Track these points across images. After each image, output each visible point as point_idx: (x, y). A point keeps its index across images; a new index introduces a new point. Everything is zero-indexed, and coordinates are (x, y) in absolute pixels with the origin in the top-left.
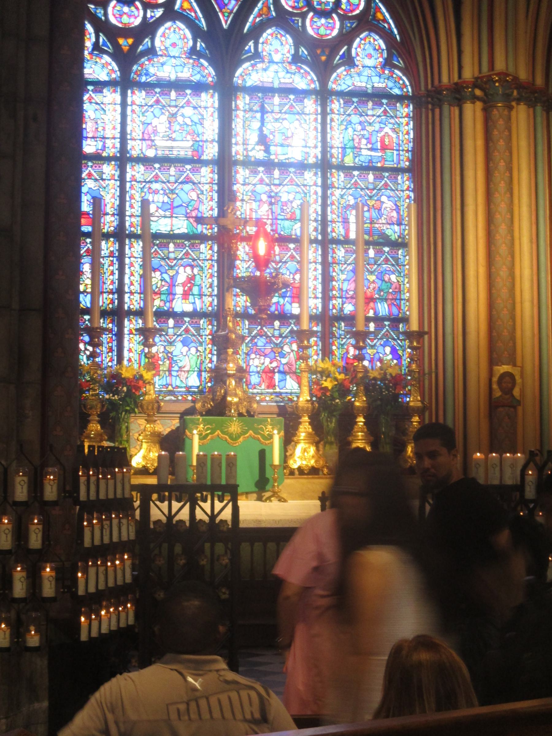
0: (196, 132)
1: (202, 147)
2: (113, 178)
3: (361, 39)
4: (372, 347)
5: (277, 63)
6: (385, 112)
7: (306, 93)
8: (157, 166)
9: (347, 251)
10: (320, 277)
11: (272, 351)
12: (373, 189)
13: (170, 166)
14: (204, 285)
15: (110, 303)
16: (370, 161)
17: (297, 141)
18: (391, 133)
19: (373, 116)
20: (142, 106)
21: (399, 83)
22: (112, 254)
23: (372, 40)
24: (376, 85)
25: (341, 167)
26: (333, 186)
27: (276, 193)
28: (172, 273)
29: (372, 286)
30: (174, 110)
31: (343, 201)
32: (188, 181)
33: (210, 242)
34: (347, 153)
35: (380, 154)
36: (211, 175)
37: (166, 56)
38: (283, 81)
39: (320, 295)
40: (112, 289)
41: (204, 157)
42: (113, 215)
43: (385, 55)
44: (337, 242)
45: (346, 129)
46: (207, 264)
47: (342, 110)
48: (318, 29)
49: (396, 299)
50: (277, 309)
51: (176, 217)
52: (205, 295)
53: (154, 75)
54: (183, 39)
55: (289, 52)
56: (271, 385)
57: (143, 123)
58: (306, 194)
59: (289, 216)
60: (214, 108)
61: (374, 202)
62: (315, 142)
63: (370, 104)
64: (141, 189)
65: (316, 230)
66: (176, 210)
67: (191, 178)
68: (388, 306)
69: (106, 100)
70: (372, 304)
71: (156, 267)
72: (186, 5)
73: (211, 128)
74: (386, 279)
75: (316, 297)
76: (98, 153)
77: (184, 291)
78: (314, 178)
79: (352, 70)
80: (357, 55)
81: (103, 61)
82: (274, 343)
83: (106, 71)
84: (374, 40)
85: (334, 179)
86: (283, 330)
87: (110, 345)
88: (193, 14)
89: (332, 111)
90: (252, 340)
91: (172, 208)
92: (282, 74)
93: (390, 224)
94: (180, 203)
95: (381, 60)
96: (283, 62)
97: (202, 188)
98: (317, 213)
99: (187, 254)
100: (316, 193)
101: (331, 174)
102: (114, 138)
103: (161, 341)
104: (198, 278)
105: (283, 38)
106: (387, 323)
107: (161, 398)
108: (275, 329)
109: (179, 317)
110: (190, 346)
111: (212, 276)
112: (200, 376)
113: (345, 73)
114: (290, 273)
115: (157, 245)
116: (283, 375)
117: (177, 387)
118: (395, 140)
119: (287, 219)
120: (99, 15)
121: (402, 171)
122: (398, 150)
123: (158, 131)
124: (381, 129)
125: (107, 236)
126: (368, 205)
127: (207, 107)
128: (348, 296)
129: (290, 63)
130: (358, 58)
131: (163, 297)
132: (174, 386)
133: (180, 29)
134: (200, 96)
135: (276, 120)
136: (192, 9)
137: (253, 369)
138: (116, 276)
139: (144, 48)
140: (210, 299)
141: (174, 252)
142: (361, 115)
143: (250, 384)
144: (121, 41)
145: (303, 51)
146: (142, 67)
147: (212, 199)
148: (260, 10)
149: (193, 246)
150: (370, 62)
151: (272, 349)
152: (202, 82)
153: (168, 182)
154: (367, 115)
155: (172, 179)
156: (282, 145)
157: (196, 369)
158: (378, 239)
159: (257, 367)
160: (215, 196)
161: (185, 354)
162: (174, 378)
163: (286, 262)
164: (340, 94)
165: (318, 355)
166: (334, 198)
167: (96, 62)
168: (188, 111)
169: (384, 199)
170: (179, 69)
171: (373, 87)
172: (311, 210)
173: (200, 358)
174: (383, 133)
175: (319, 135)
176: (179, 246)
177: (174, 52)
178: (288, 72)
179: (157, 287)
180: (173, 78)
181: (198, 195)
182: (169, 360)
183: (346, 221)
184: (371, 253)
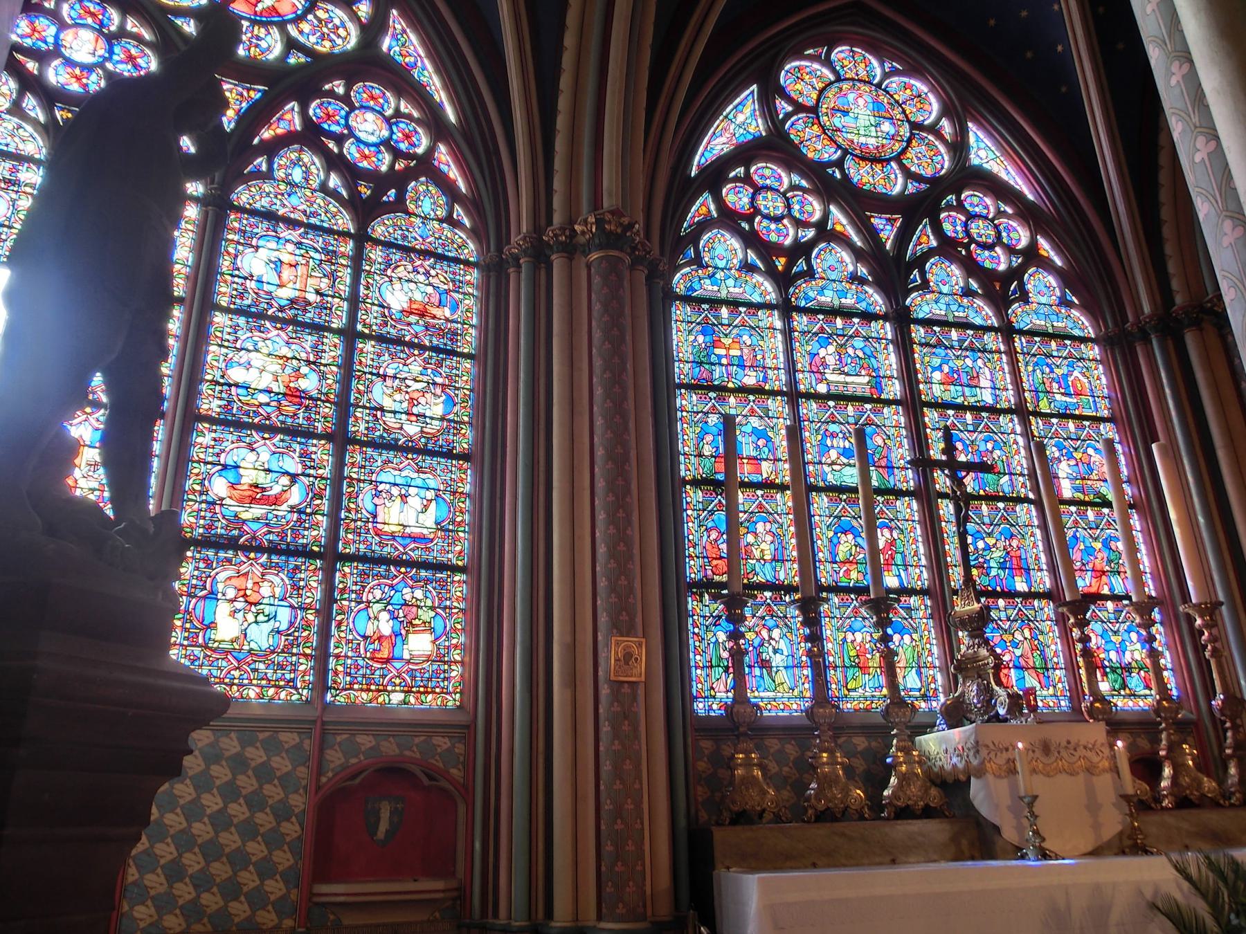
10: (1040, 544)
14: (907, 553)
17: (984, 382)
21: (1079, 322)
25: (1037, 414)
39: (1045, 567)
45: (1034, 371)
65: (1024, 485)
72: (838, 228)
75: (1040, 570)
86: (1009, 612)
100: (1016, 442)
107: (874, 705)
124: (1070, 373)
140: (917, 571)
145: (974, 285)
147: (901, 446)
155: (851, 420)
156: (968, 386)
169: (1090, 451)
184: (1091, 514)
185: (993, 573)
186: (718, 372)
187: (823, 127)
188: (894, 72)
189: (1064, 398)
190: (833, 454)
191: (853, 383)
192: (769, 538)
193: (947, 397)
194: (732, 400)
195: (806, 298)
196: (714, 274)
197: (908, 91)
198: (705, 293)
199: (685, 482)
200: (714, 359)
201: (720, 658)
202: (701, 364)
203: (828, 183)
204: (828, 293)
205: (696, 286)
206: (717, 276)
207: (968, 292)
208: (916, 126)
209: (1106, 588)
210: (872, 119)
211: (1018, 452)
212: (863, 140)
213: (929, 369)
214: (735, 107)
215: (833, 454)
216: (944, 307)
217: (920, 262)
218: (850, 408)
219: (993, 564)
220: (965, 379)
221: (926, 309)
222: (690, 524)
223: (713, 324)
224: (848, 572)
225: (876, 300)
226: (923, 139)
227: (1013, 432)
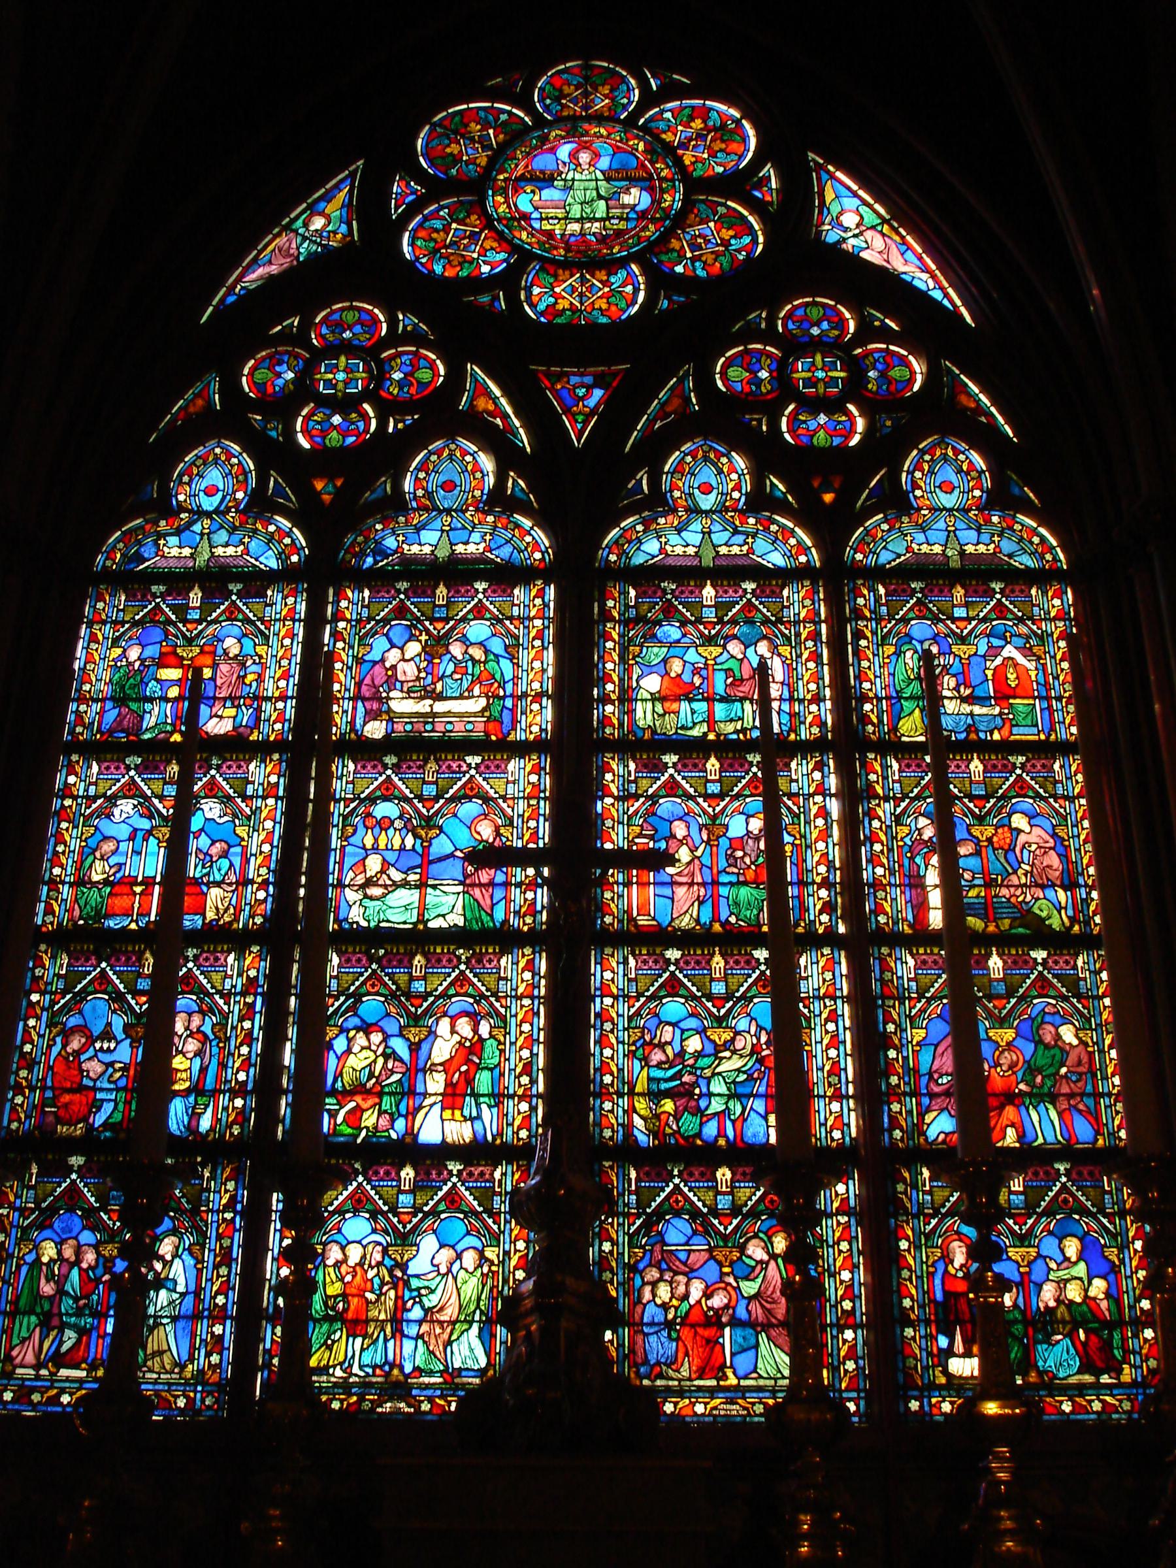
0: (498, 676)
1: (513, 711)
2: (270, 791)
3: (922, 452)
4: (1023, 1240)
5: (707, 513)
6: (1000, 611)
8: (390, 760)
9: (921, 964)
11: (712, 1257)
12: (986, 798)
13: (426, 761)
15: (234, 1122)
16: (970, 729)
18: (1021, 659)
19: (968, 619)
20: (359, 621)
21: (1031, 541)
23: (950, 453)
24: (970, 549)
26: (870, 793)
27: (714, 818)
28: (414, 1034)
29: (1006, 1058)
31: (903, 831)
32: (470, 793)
33: (528, 951)
34: (906, 711)
35: (997, 710)
36: (534, 778)
37: (426, 509)
38: (723, 550)
40: (245, 1083)
41: (520, 735)
42: (264, 885)
43: (987, 482)
44: (896, 940)
45: (898, 653)
47: (884, 609)
48: (812, 437)
49: (1083, 1094)
50: (721, 1132)
51: (434, 887)
52: (512, 1097)
53: (396, 552)
54: (473, 472)
55: (738, 487)
56: (712, 1366)
57: (359, 661)
58: (798, 817)
59: (750, 875)
60: (543, 618)
61: (990, 831)
62: (813, 686)
63: (959, 592)
64: (345, 818)
65: (828, 907)
66: (434, 869)
67: (480, 787)
68: (1060, 1114)
70: (1010, 1112)
71: (371, 1020)
72: (482, 404)
73: (539, 666)
74: (1048, 1038)
75: (838, 1096)
76: (240, 734)
77: (449, 1084)
78: (817, 775)
79: (905, 519)
80: (915, 486)
81: (272, 528)
82: (717, 1232)
83: (276, 548)
84: (957, 452)
85: (873, 777)
87: (226, 1242)
88: (498, 421)
89: (858, 614)
90: (648, 1226)
91: (426, 861)
92: (720, 537)
93: (1043, 887)
94: (449, 848)
95: (977, 493)
96: (721, 509)
97: (509, 811)
98: (830, 865)
99: (462, 980)
100: (824, 812)
101: (864, 764)
102: (283, 698)
103: (374, 1231)
104: (490, 1045)
105: (724, 460)
106: (1061, 1167)
107: (366, 1405)
108: (718, 1193)
110: (459, 1247)
111: (530, 1041)
112: (487, 1337)
113: (885, 527)
114: (760, 1028)
115: (379, 961)
116: (749, 1331)
117: (418, 1370)
118: (1033, 674)
119: (745, 883)
120: (274, 434)
121: (1065, 748)
122: (1048, 698)
123: (400, 677)
124: (993, 652)
125: (239, 940)
126: (977, 842)
127: (530, 619)
128: (936, 1089)
130: (918, 493)
132: (408, 1368)
133: (465, 453)
134: (511, 595)
135: (709, 641)
137: (651, 1312)
138: (258, 1047)
139: (374, 496)
140: (524, 1107)
141: (424, 978)
142: (936, 620)
143: (646, 1361)
144: (319, 485)
146: (367, 539)
148: (663, 405)
149: (479, 961)
150: (948, 500)
151: (710, 1250)
152: (517, 562)
153: (420, 798)
154: (954, 620)
155: (430, 790)
156: (723, 700)
157: (477, 1318)
158: (1011, 927)
159: (665, 1307)
161: (443, 1270)
162: (408, 1345)
163: (746, 999)
164: (878, 574)
165: (853, 1268)
166: (876, 824)
167: (255, 531)
168: (478, 630)
169: (1019, 821)
170: (455, 536)
171: (962, 553)
172: (812, 859)
173: (490, 1281)
174: (999, 660)
175: (826, 668)
176: (439, 961)
178: (736, 532)
179: (371, 1075)
180: (443, 553)
181: (497, 829)
182: (395, 1287)
183: (915, 883)
184: (995, 963)
188: (670, 91)
189: (966, 708)
191: (448, 714)
193: (669, 726)
196: (191, 523)
197: (698, 124)
198: (163, 563)
199: (39, 935)
200: (152, 688)
201: (37, 1296)
202: (120, 700)
203: (472, 322)
204: (430, 536)
205: (148, 551)
206: (197, 528)
207: (759, 502)
208: (696, 186)
209: (1011, 1133)
210: (603, 184)
211: (825, 835)
213: (637, 671)
214: (310, 207)
215: (374, 864)
216: (696, 539)
217: (654, 451)
218: (432, 766)
219: (718, 1087)
220: (720, 684)
221: (652, 546)
222: (32, 1022)
223: (169, 622)
224: (358, 1111)
227: (821, 790)
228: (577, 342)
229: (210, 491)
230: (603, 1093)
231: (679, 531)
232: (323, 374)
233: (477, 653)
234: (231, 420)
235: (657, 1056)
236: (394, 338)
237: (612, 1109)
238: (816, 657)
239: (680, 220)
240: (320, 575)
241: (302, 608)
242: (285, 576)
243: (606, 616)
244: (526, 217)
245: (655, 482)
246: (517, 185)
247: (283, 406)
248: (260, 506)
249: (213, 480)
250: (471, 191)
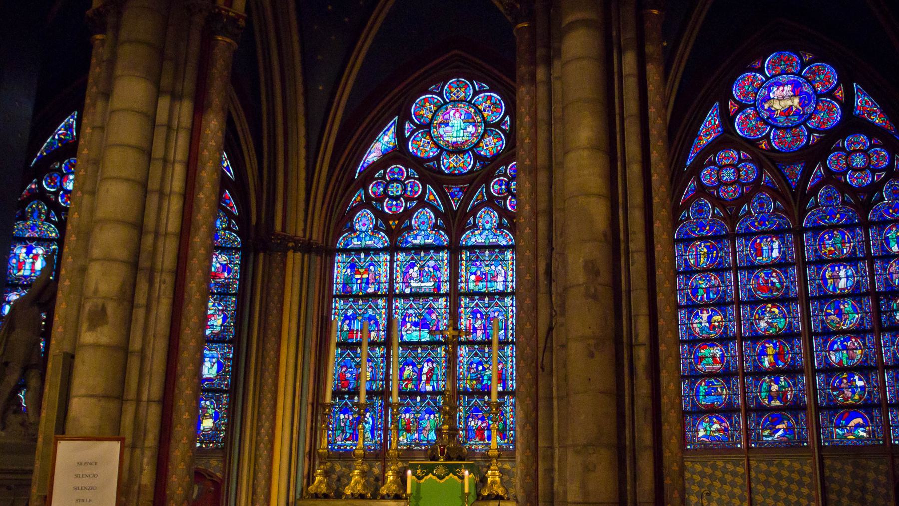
2: (384, 307)
7: (506, 247)
17: (501, 279)
22: (382, 356)
30: (422, 263)
41: (441, 292)
46: (442, 360)
65: (512, 335)
69: (381, 260)
72: (431, 197)
73: (445, 274)
75: (512, 380)
96: (491, 229)
99: (429, 354)
100: (512, 311)
109: (423, 394)
125: (379, 345)
129: (496, 229)
131: (414, 382)
135: (487, 266)
136: (435, 200)
144: (391, 222)
145: (505, 220)
155: (421, 307)
160: (447, 316)
168: (431, 263)
177: (423, 227)
180: (422, 242)
185: (485, 382)
186: (355, 288)
187: (431, 138)
190: (408, 325)
192: (370, 370)
193: (476, 289)
194: (360, 302)
195: (407, 242)
197: (489, 102)
203: (428, 172)
204: (419, 237)
208: (487, 124)
212: (455, 140)
225: (444, 239)
226: (492, 131)
228: (455, 177)
229: (364, 225)
230: (461, 379)
231: (481, 234)
232: (390, 189)
233: (431, 270)
234: (367, 203)
235: (472, 371)
236: (408, 177)
237: (463, 383)
238: (512, 270)
239: (483, 137)
240: (392, 249)
241: (388, 258)
242: (384, 249)
243: (462, 259)
244: (442, 136)
245: (475, 221)
246: (440, 125)
247: (380, 199)
248: (376, 229)
249: (364, 220)
250: (426, 127)
